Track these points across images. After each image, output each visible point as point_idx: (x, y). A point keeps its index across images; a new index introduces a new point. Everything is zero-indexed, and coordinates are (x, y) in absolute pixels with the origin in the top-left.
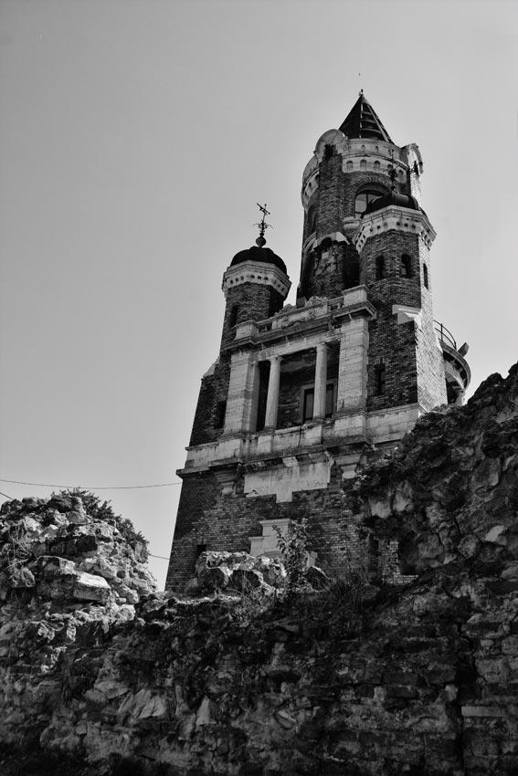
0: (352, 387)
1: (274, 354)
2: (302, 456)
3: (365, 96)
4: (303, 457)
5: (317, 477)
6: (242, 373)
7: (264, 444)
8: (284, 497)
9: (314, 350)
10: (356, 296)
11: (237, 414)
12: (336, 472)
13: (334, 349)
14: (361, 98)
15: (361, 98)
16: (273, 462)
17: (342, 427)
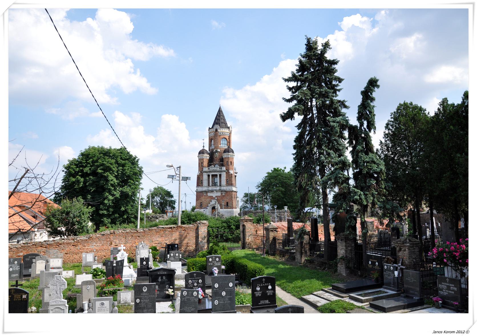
0: (224, 182)
1: (211, 174)
2: (216, 191)
3: (221, 107)
4: (216, 191)
5: (219, 194)
6: (205, 176)
7: (210, 188)
8: (214, 196)
9: (217, 175)
10: (224, 168)
11: (205, 183)
12: (222, 194)
13: (220, 175)
14: (220, 108)
15: (220, 108)
16: (212, 191)
17: (222, 188)
